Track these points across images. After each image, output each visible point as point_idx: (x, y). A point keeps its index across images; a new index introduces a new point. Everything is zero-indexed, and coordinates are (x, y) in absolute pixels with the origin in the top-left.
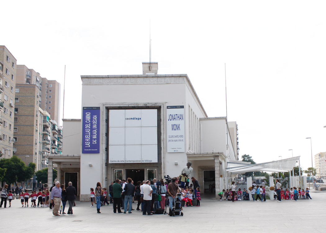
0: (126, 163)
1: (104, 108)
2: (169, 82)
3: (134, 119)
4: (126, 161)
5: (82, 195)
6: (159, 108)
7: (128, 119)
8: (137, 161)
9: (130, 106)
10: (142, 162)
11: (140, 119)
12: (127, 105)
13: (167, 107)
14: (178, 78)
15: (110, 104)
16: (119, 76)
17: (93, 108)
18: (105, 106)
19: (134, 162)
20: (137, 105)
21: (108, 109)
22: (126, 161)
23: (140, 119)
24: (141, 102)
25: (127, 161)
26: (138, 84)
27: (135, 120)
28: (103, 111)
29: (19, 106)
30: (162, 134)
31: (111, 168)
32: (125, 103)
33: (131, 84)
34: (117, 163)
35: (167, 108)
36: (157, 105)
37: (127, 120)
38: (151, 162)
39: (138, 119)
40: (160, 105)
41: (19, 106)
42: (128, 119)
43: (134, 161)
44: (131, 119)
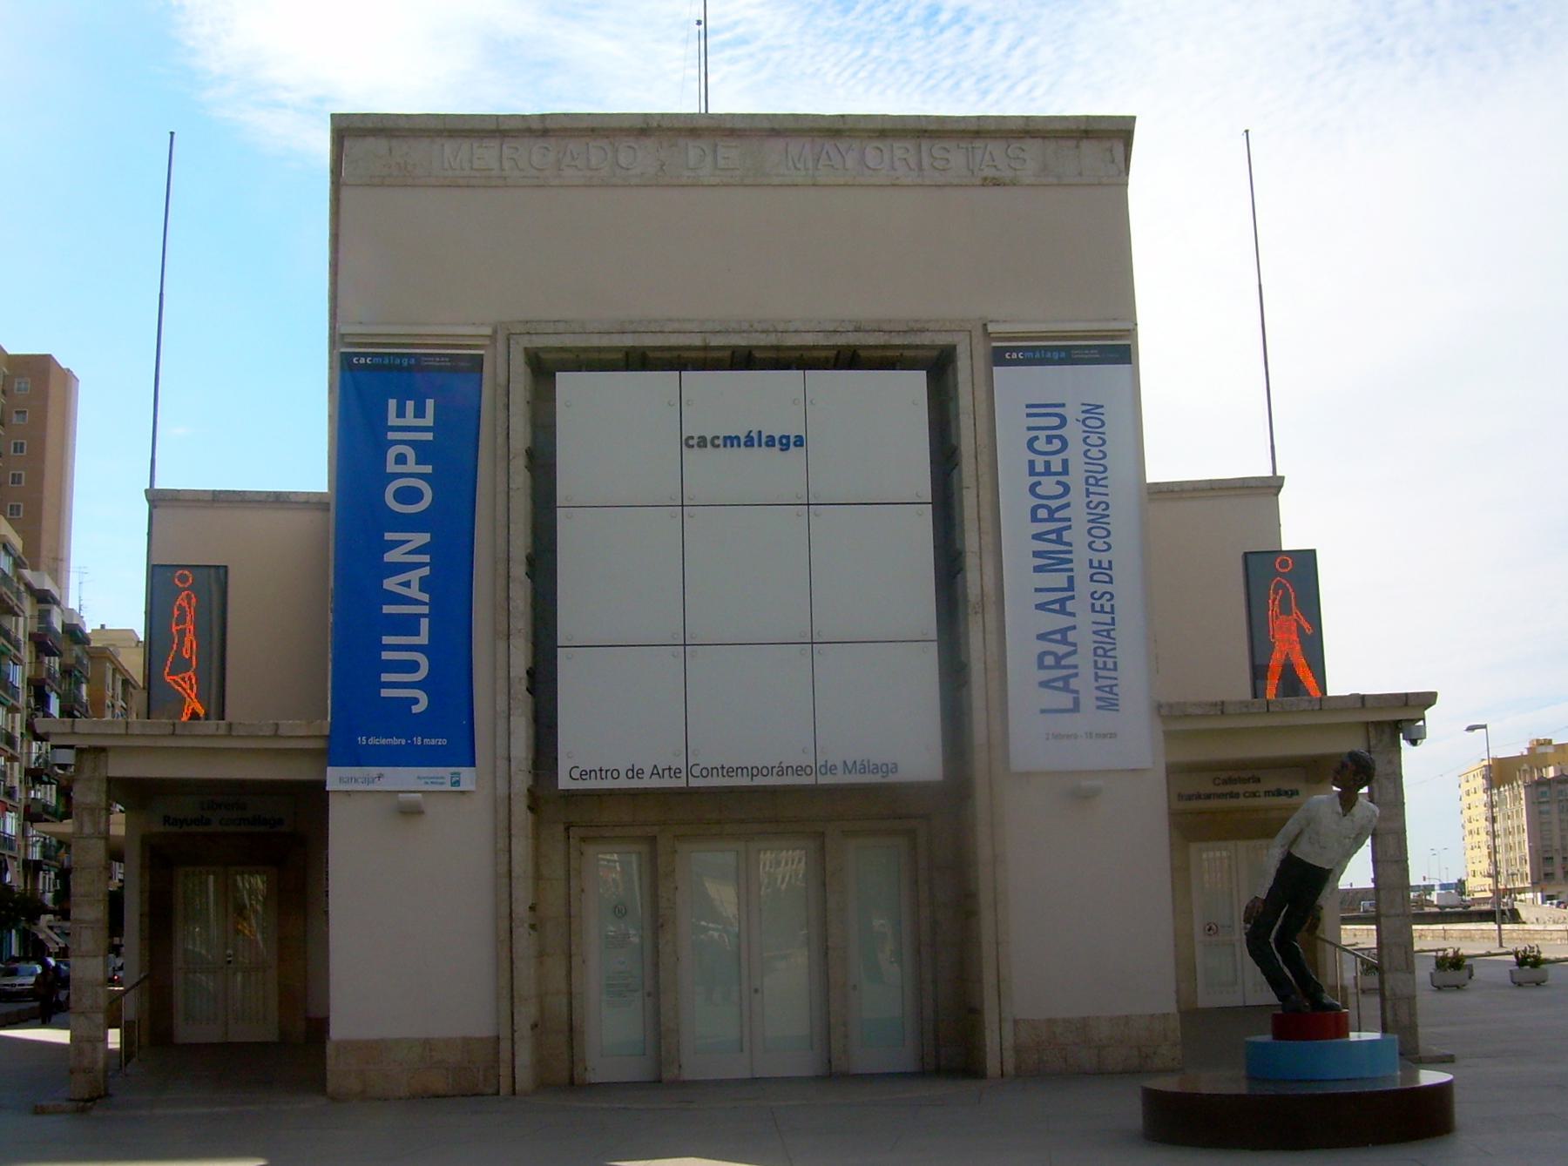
0: (694, 783)
1: (519, 361)
2: (1007, 174)
3: (749, 442)
4: (696, 771)
5: (347, 1046)
7: (702, 442)
8: (782, 771)
9: (715, 341)
10: (822, 780)
11: (800, 442)
12: (697, 341)
14: (1072, 143)
15: (561, 327)
16: (626, 124)
18: (526, 342)
19: (759, 781)
20: (772, 340)
22: (696, 771)
23: (800, 442)
25: (709, 771)
26: (776, 181)
27: (760, 453)
30: (971, 561)
31: (561, 827)
32: (676, 326)
33: (717, 180)
34: (623, 783)
36: (925, 339)
38: (892, 778)
39: (785, 447)
40: (942, 340)
42: (702, 442)
43: (755, 771)
44: (731, 441)
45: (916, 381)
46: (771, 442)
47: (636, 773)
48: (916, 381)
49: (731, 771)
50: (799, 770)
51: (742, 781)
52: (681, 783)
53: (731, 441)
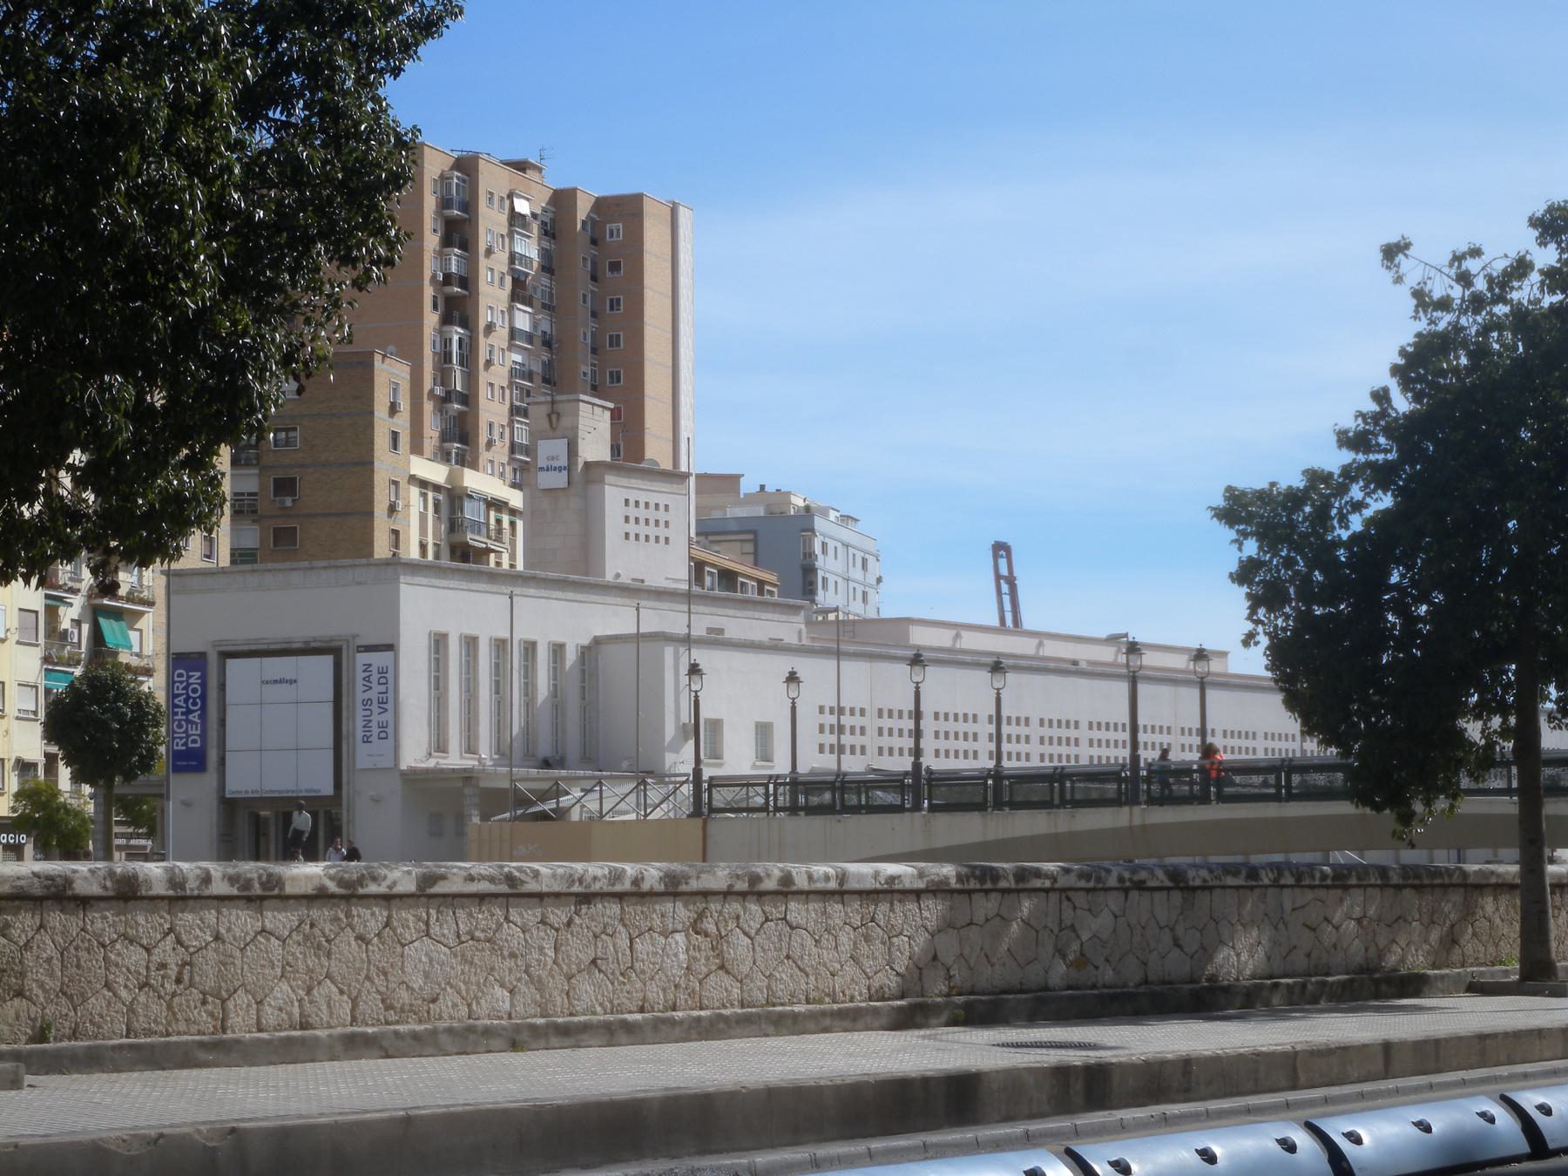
6: (336, 652)
8: (288, 792)
11: (295, 681)
13: (358, 647)
17: (192, 656)
21: (226, 655)
23: (295, 681)
24: (298, 632)
25: (267, 792)
27: (285, 685)
28: (213, 660)
29: (303, 466)
35: (358, 652)
37: (266, 687)
40: (338, 643)
41: (303, 466)
43: (279, 792)
44: (275, 682)
45: (327, 661)
46: (287, 682)
47: (247, 792)
48: (327, 661)
49: (274, 792)
50: (293, 792)
51: (276, 795)
52: (258, 795)
53: (275, 682)
